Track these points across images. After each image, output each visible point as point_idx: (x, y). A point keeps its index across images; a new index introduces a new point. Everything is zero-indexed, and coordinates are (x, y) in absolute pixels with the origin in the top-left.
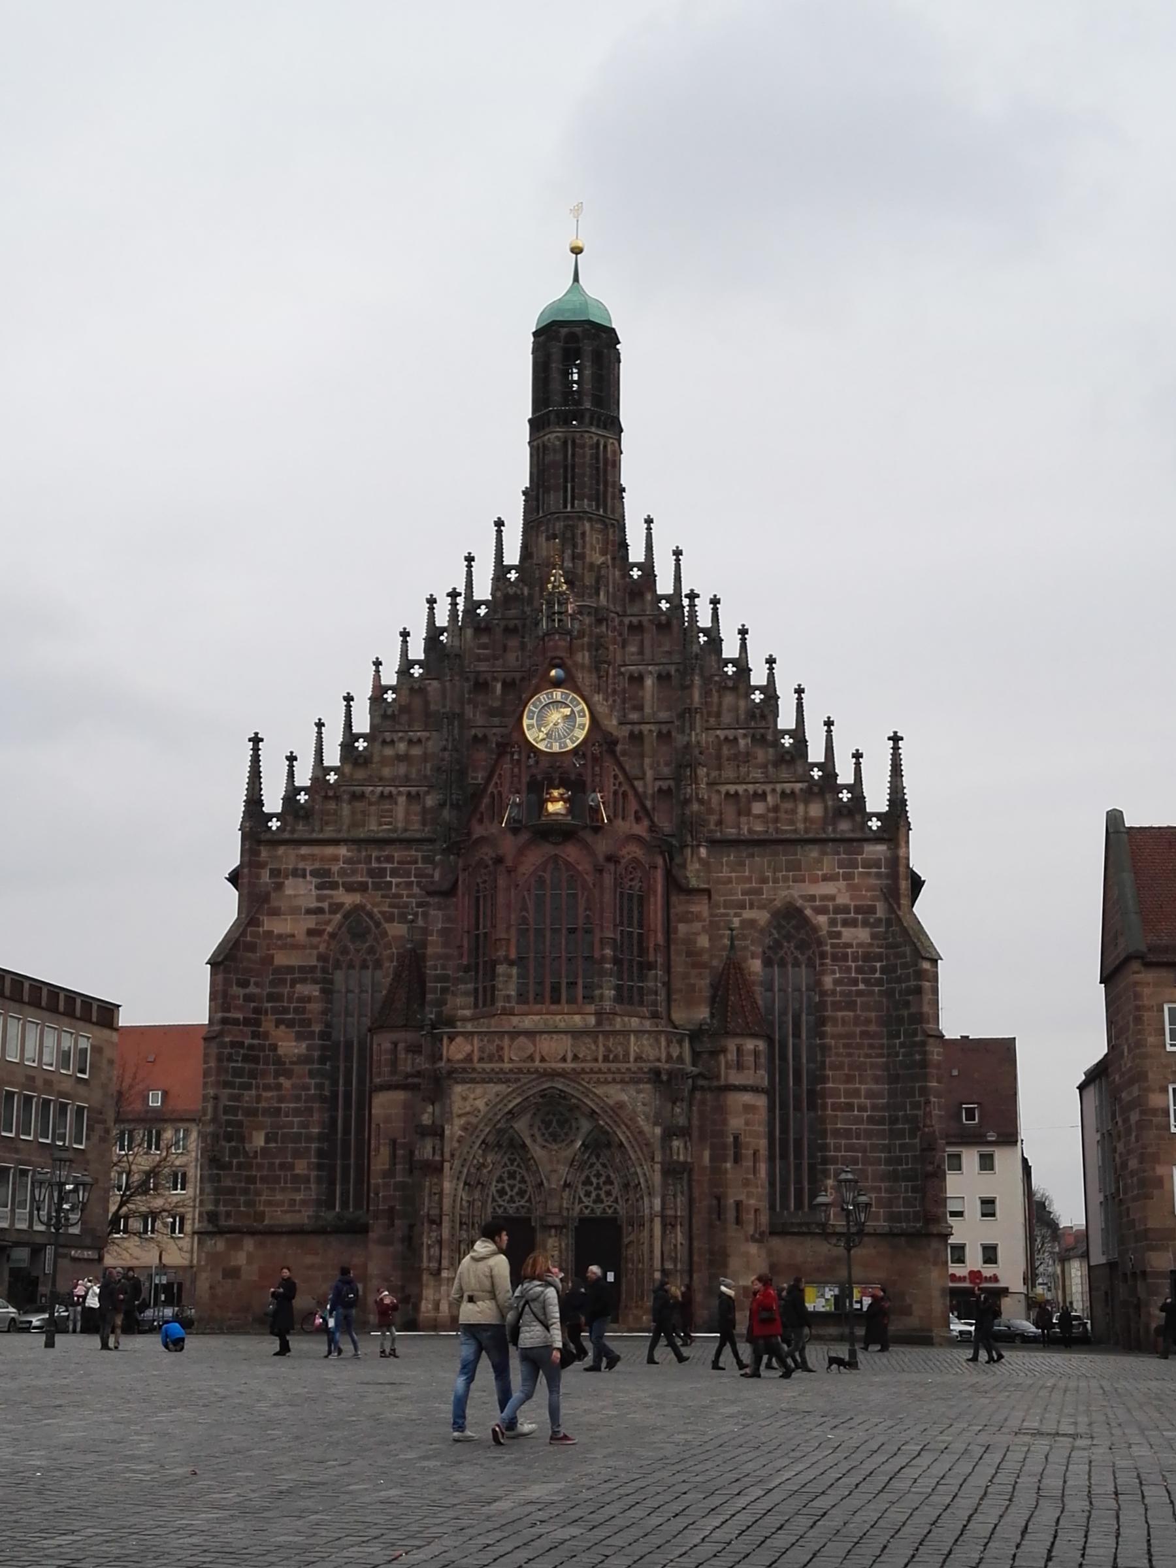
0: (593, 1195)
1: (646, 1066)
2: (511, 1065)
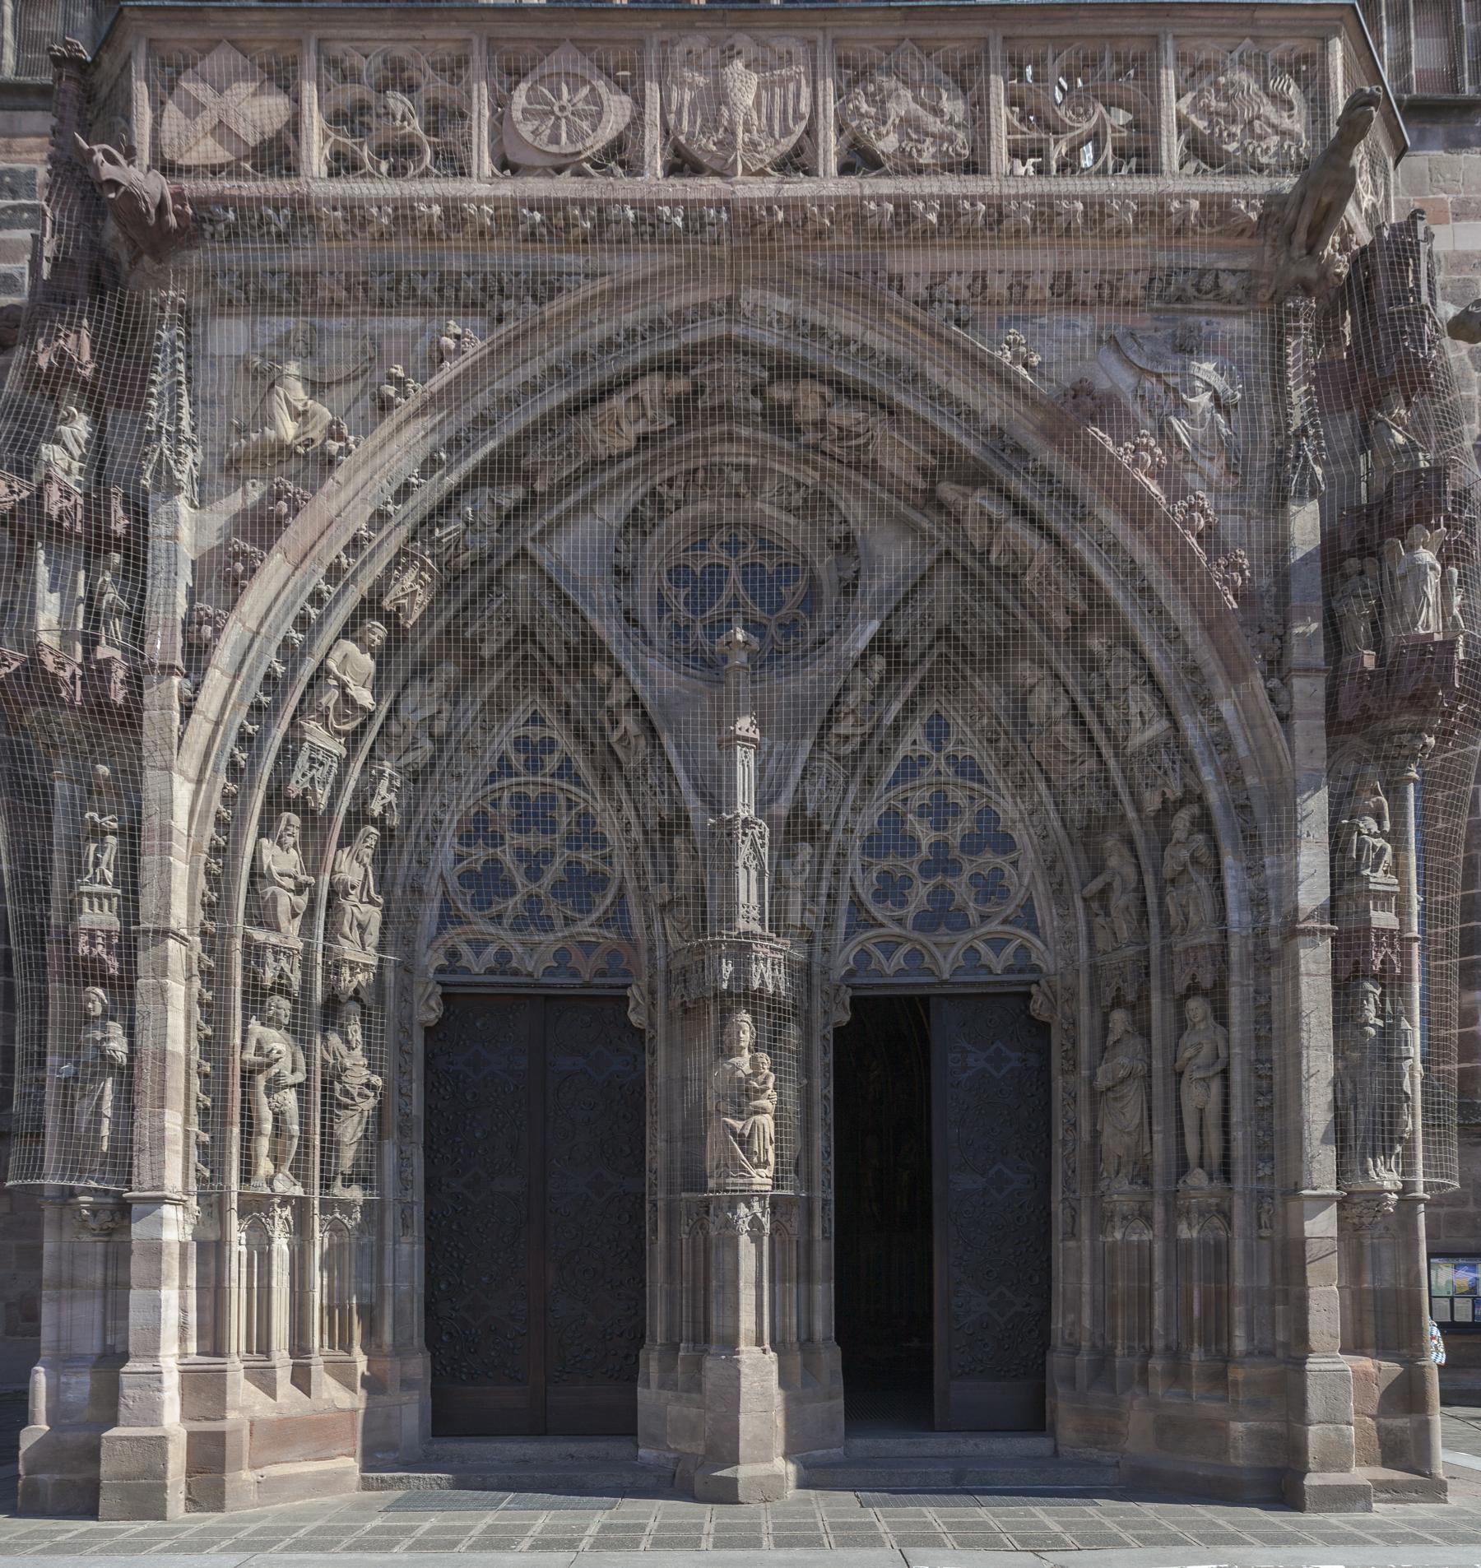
0: (920, 894)
1: (1248, 191)
2: (508, 188)
